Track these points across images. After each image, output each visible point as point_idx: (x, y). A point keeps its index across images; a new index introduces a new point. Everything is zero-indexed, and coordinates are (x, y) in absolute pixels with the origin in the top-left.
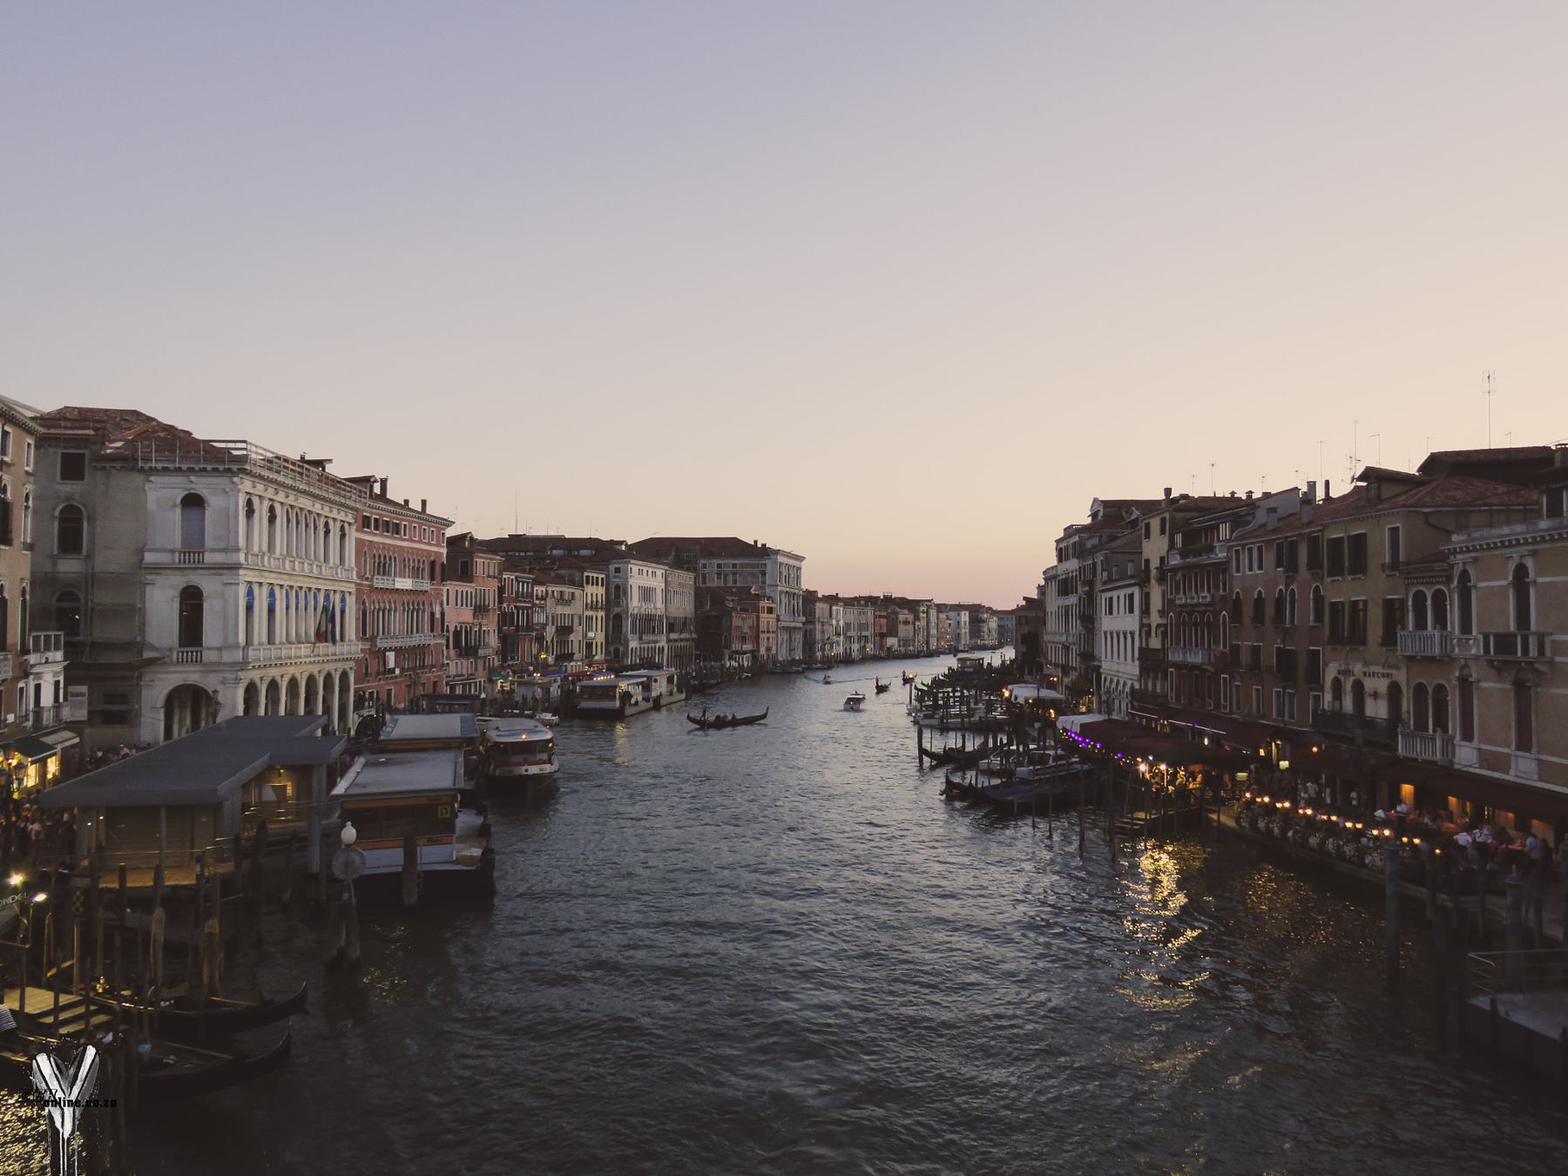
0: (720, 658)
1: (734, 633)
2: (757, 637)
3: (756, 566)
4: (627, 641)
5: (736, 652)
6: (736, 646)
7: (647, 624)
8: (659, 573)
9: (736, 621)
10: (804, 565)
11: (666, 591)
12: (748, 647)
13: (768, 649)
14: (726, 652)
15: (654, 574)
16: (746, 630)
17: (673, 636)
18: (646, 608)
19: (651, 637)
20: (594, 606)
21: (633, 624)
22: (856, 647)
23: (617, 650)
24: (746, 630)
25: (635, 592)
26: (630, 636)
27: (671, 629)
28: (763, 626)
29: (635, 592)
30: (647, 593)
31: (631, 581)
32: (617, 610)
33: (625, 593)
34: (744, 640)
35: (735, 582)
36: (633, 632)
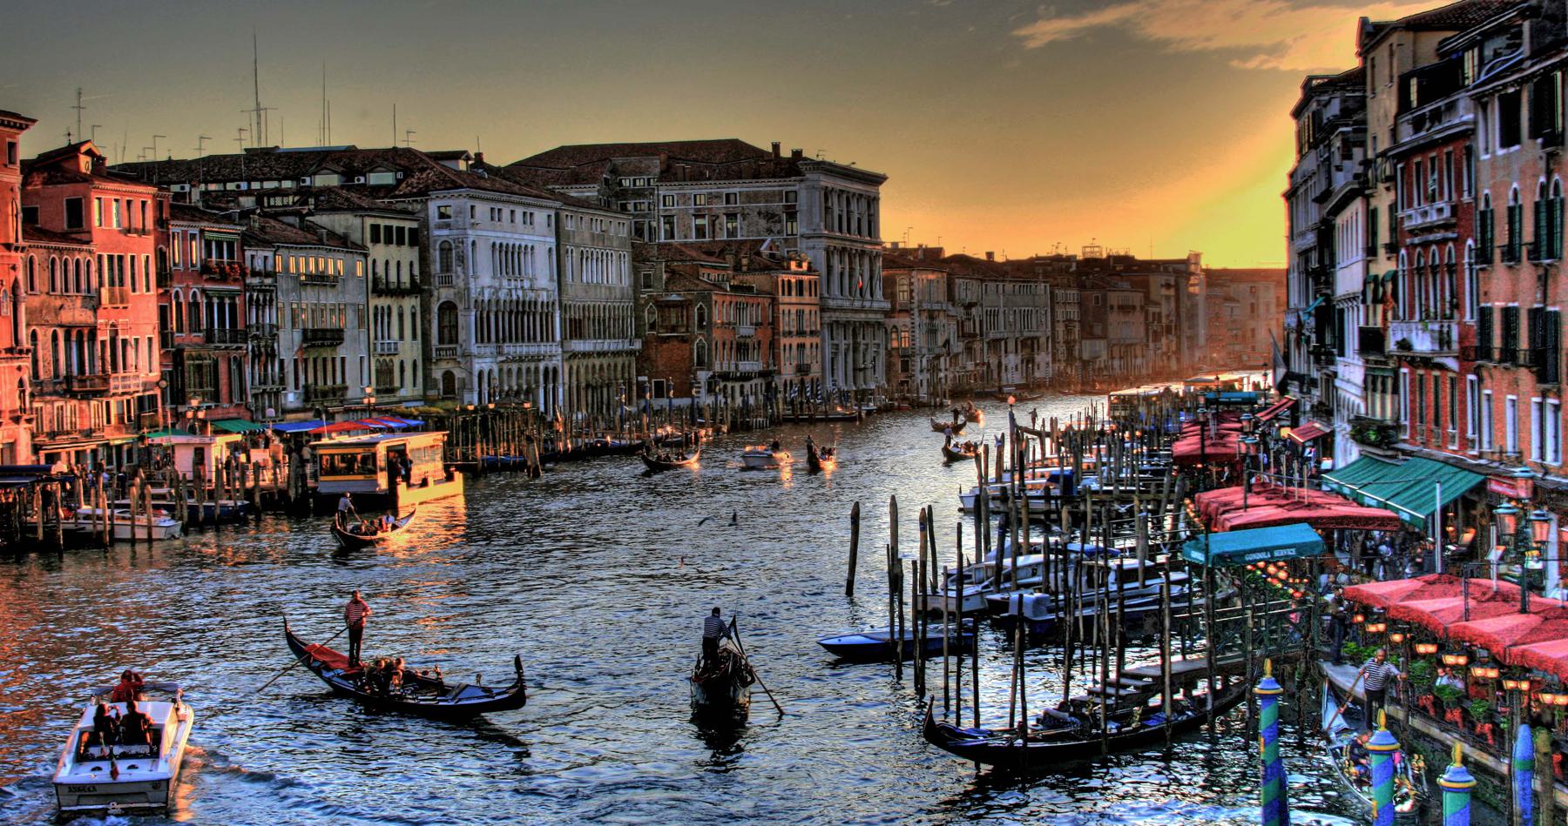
2: (773, 345)
3: (768, 197)
5: (725, 376)
6: (723, 363)
7: (516, 320)
8: (540, 216)
10: (884, 191)
13: (802, 369)
15: (528, 219)
16: (746, 330)
17: (578, 346)
21: (482, 323)
22: (1012, 360)
27: (575, 329)
28: (787, 323)
33: (462, 259)
34: (742, 349)
35: (732, 233)
36: (482, 338)
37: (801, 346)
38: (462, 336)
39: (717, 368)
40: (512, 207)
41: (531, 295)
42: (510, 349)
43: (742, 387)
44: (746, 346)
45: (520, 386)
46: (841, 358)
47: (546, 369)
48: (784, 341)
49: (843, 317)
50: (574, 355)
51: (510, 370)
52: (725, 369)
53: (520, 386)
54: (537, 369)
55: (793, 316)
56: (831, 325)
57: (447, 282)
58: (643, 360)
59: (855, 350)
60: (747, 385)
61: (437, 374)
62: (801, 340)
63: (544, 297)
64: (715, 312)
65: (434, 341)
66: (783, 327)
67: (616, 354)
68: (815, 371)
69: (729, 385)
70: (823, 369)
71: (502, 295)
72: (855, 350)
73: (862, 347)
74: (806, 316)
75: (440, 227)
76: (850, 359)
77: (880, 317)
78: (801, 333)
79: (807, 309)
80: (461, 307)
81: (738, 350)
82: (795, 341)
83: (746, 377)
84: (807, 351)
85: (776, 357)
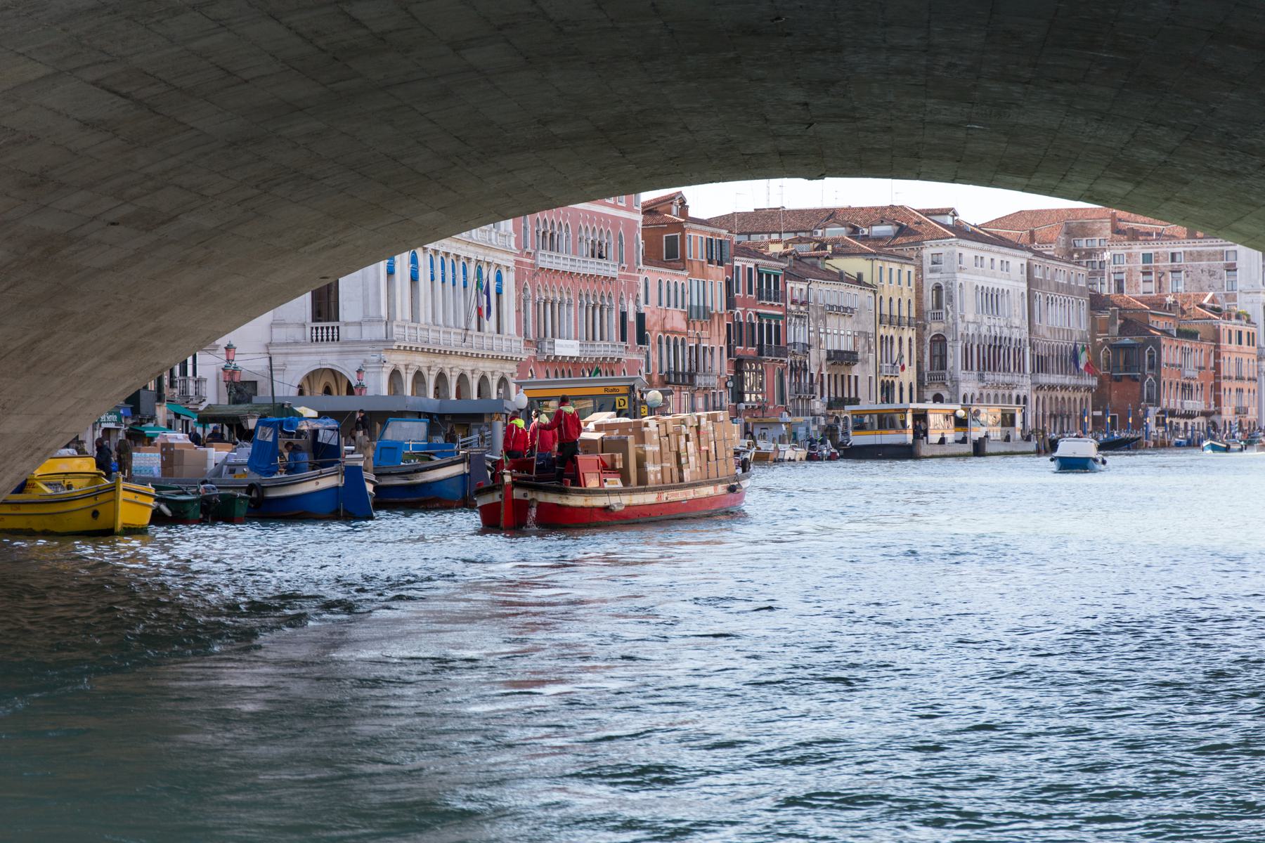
1: (1165, 377)
2: (1217, 387)
4: (956, 383)
5: (1172, 413)
6: (1171, 400)
9: (1170, 353)
11: (1031, 297)
13: (1240, 411)
18: (991, 326)
19: (1001, 377)
20: (894, 321)
21: (967, 352)
25: (969, 294)
26: (960, 374)
28: (1228, 368)
29: (969, 294)
30: (991, 300)
31: (961, 278)
32: (935, 327)
33: (951, 299)
34: (1186, 389)
37: (1240, 391)
38: (950, 363)
40: (992, 256)
41: (1006, 333)
42: (989, 376)
43: (1186, 424)
48: (1225, 384)
52: (1172, 406)
54: (1010, 396)
55: (1233, 361)
57: (937, 318)
60: (1190, 422)
62: (1239, 384)
63: (1016, 335)
64: (1164, 354)
65: (927, 368)
66: (1224, 371)
71: (984, 330)
74: (1245, 363)
75: (932, 271)
79: (1245, 358)
80: (949, 339)
81: (1183, 390)
83: (1190, 415)
84: (1245, 393)
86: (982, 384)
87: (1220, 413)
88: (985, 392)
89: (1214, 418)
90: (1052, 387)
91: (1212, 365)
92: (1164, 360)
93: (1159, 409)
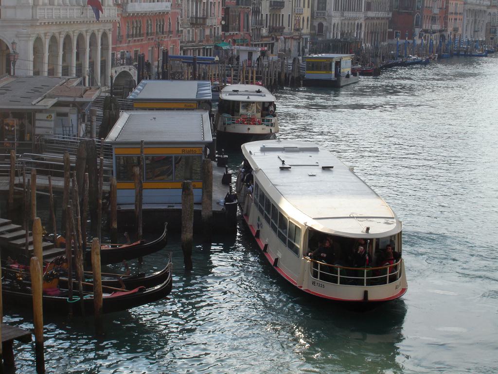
0: (412, 36)
2: (446, 18)
5: (426, 31)
6: (426, 25)
12: (436, 27)
13: (456, 30)
14: (417, 31)
16: (436, 11)
17: (371, 14)
23: (321, 25)
24: (436, 11)
26: (333, 13)
28: (451, 9)
34: (433, 19)
36: (336, 9)
37: (456, 19)
38: (328, 7)
39: (424, 28)
42: (346, 14)
44: (435, 17)
45: (348, 31)
46: (470, 25)
47: (358, 24)
48: (450, 17)
49: (472, 7)
50: (367, 18)
51: (345, 23)
52: (427, 28)
53: (348, 31)
54: (355, 23)
55: (454, 5)
56: (467, 11)
58: (392, 22)
59: (475, 22)
61: (316, 24)
65: (315, 9)
67: (383, 18)
68: (460, 32)
69: (427, 35)
70: (463, 30)
72: (475, 22)
73: (478, 21)
74: (458, 5)
76: (473, 27)
77: (485, 8)
78: (456, 13)
81: (432, 20)
82: (453, 17)
83: (434, 32)
84: (458, 21)
85: (446, 24)
86: (342, 18)
87: (447, 31)
88: (343, 22)
89: (444, 33)
90: (373, 18)
91: (445, 7)
92: (425, 5)
93: (421, 29)
